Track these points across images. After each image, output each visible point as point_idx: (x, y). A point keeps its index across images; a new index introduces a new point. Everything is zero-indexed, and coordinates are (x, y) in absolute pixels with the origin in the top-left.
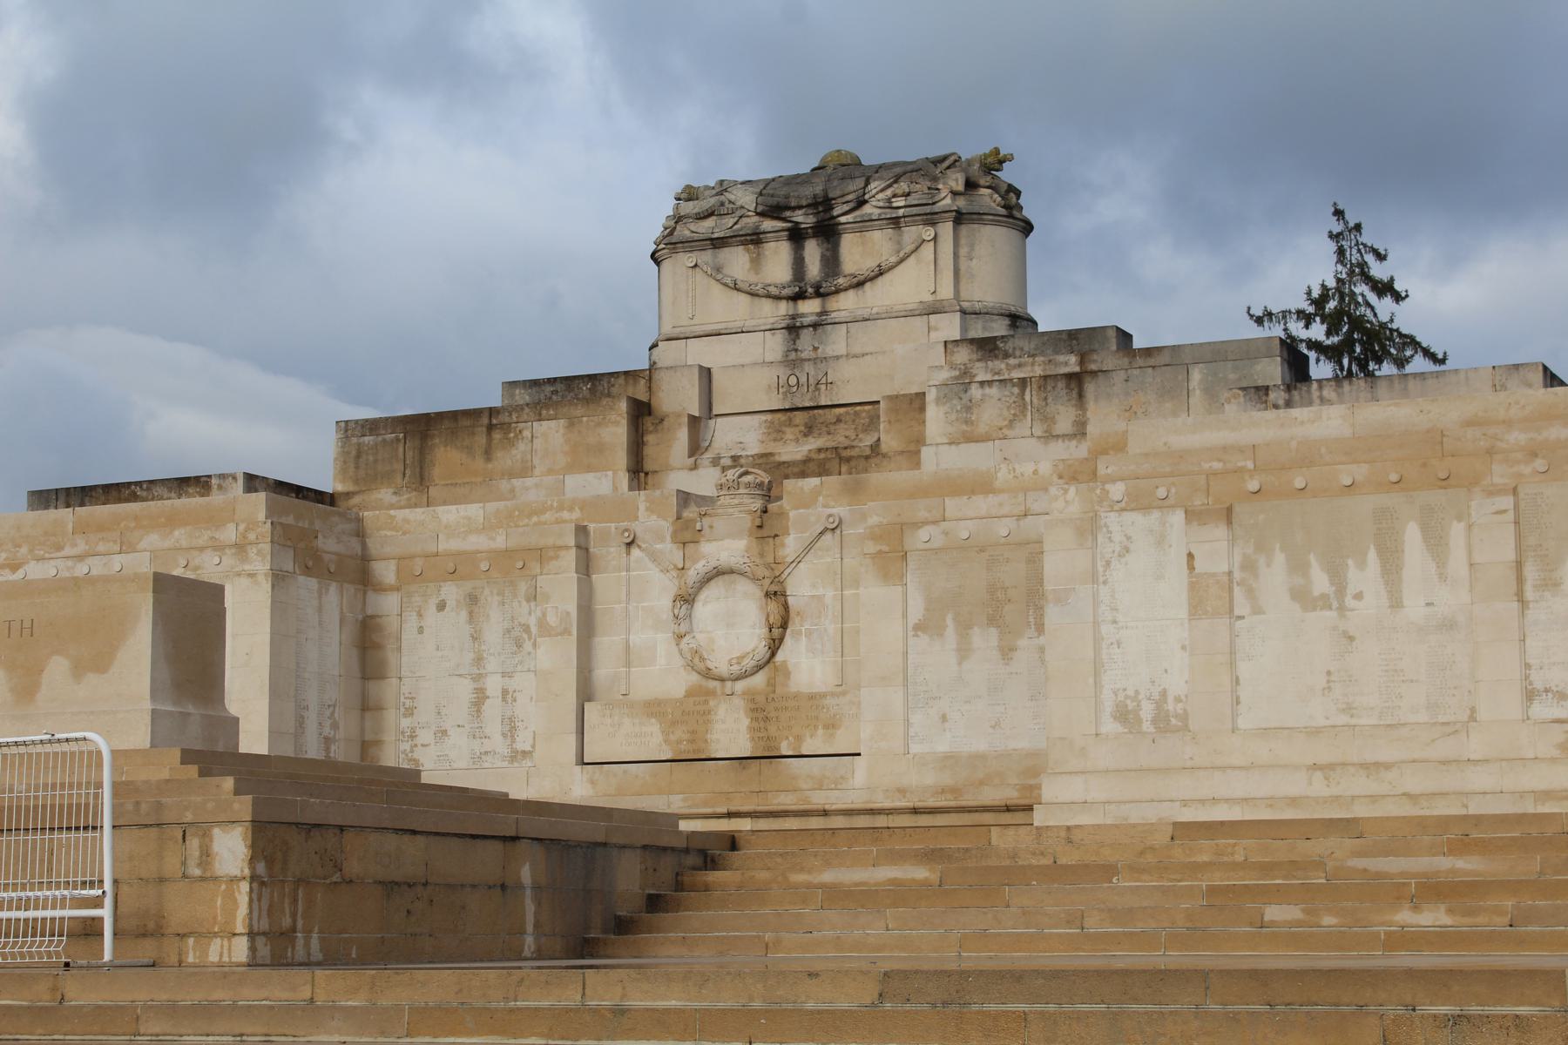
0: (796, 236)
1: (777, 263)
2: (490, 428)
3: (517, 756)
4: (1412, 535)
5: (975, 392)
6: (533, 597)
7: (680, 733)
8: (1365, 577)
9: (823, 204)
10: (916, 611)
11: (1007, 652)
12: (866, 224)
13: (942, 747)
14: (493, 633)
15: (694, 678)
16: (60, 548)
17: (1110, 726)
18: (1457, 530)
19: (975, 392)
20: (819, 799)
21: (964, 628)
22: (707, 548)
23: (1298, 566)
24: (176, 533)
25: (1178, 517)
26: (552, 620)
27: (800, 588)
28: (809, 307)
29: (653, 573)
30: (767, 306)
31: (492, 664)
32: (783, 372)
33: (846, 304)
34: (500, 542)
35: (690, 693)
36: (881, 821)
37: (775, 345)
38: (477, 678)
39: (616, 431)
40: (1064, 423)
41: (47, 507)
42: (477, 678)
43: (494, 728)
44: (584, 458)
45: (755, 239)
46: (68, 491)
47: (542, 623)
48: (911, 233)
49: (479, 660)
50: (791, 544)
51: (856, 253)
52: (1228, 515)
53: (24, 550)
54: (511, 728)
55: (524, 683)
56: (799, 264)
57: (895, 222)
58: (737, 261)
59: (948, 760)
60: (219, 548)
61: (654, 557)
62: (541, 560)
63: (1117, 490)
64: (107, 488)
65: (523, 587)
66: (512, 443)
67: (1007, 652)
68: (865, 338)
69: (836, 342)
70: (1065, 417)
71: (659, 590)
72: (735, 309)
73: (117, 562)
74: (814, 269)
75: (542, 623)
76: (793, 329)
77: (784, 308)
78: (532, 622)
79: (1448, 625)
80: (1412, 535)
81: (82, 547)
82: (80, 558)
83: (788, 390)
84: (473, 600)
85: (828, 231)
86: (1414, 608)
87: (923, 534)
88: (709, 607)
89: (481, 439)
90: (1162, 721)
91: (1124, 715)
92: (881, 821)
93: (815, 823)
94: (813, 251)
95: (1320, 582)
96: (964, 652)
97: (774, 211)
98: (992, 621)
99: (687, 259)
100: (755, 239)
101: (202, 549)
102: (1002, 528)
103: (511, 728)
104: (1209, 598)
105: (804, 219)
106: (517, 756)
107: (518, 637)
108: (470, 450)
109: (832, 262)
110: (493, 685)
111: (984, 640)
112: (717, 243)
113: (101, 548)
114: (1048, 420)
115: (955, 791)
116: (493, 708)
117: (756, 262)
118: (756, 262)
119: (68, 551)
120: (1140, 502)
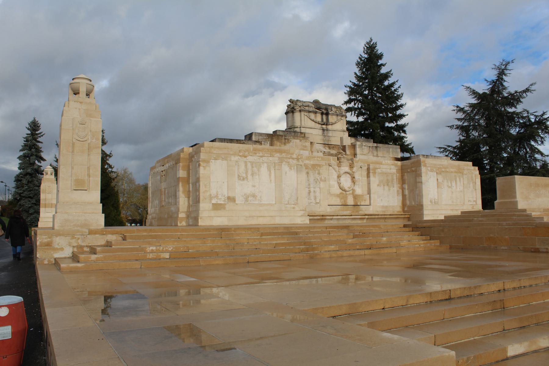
0: (322, 114)
1: (319, 118)
2: (285, 139)
3: (317, 203)
4: (458, 179)
5: (363, 147)
6: (319, 174)
7: (342, 200)
8: (454, 184)
9: (326, 109)
10: (377, 183)
11: (389, 190)
12: (333, 114)
13: (382, 204)
14: (312, 179)
15: (341, 191)
16: (256, 154)
17: (430, 203)
18: (462, 179)
19: (363, 147)
20: (367, 213)
21: (384, 185)
22: (342, 168)
23: (448, 182)
24: (283, 154)
25: (435, 173)
26: (323, 178)
27: (357, 176)
28: (324, 126)
29: (334, 171)
30: (317, 125)
31: (312, 186)
32: (323, 137)
33: (330, 127)
34: (312, 163)
35: (341, 193)
36: (373, 217)
37: (320, 132)
38: (309, 188)
39: (308, 144)
40: (375, 154)
41: (222, 142)
42: (309, 188)
43: (312, 198)
44: (304, 148)
45: (316, 113)
46: (227, 139)
47: (321, 179)
48: (339, 117)
49: (309, 185)
50: (355, 169)
51: (332, 119)
52: (441, 174)
53: (247, 153)
54: (315, 198)
55: (317, 190)
56: (322, 119)
57: (337, 115)
58: (312, 116)
59: (383, 207)
60: (293, 159)
61: (334, 169)
62: (320, 167)
63: (429, 168)
64: (237, 140)
65: (317, 172)
66: (289, 142)
67: (389, 190)
68: (335, 134)
69: (330, 134)
70: (375, 154)
71: (335, 176)
72: (312, 124)
73: (271, 159)
74: (325, 120)
75: (321, 179)
76: (323, 130)
77: (320, 126)
78: (319, 178)
79: (461, 191)
80: (458, 179)
81: (261, 154)
82: (262, 157)
83: (324, 141)
84: (308, 173)
85: (327, 114)
86: (458, 189)
87: (379, 170)
88: (342, 179)
89: (284, 141)
90: (435, 202)
91: (431, 202)
92: (385, 216)
93: (377, 217)
94: (324, 117)
95: (450, 185)
96: (384, 189)
97: (319, 109)
98: (388, 185)
99: (306, 114)
100: (316, 113)
101: (289, 158)
102: (389, 171)
103: (315, 198)
104: (439, 186)
105: (325, 111)
106: (317, 203)
107: (316, 181)
108: (281, 142)
109: (327, 119)
110: (312, 190)
111: (386, 188)
112: (309, 112)
113: (266, 155)
114: (373, 153)
115: (383, 211)
116: (312, 194)
117: (316, 117)
118: (316, 117)
119: (258, 155)
120: (432, 171)
